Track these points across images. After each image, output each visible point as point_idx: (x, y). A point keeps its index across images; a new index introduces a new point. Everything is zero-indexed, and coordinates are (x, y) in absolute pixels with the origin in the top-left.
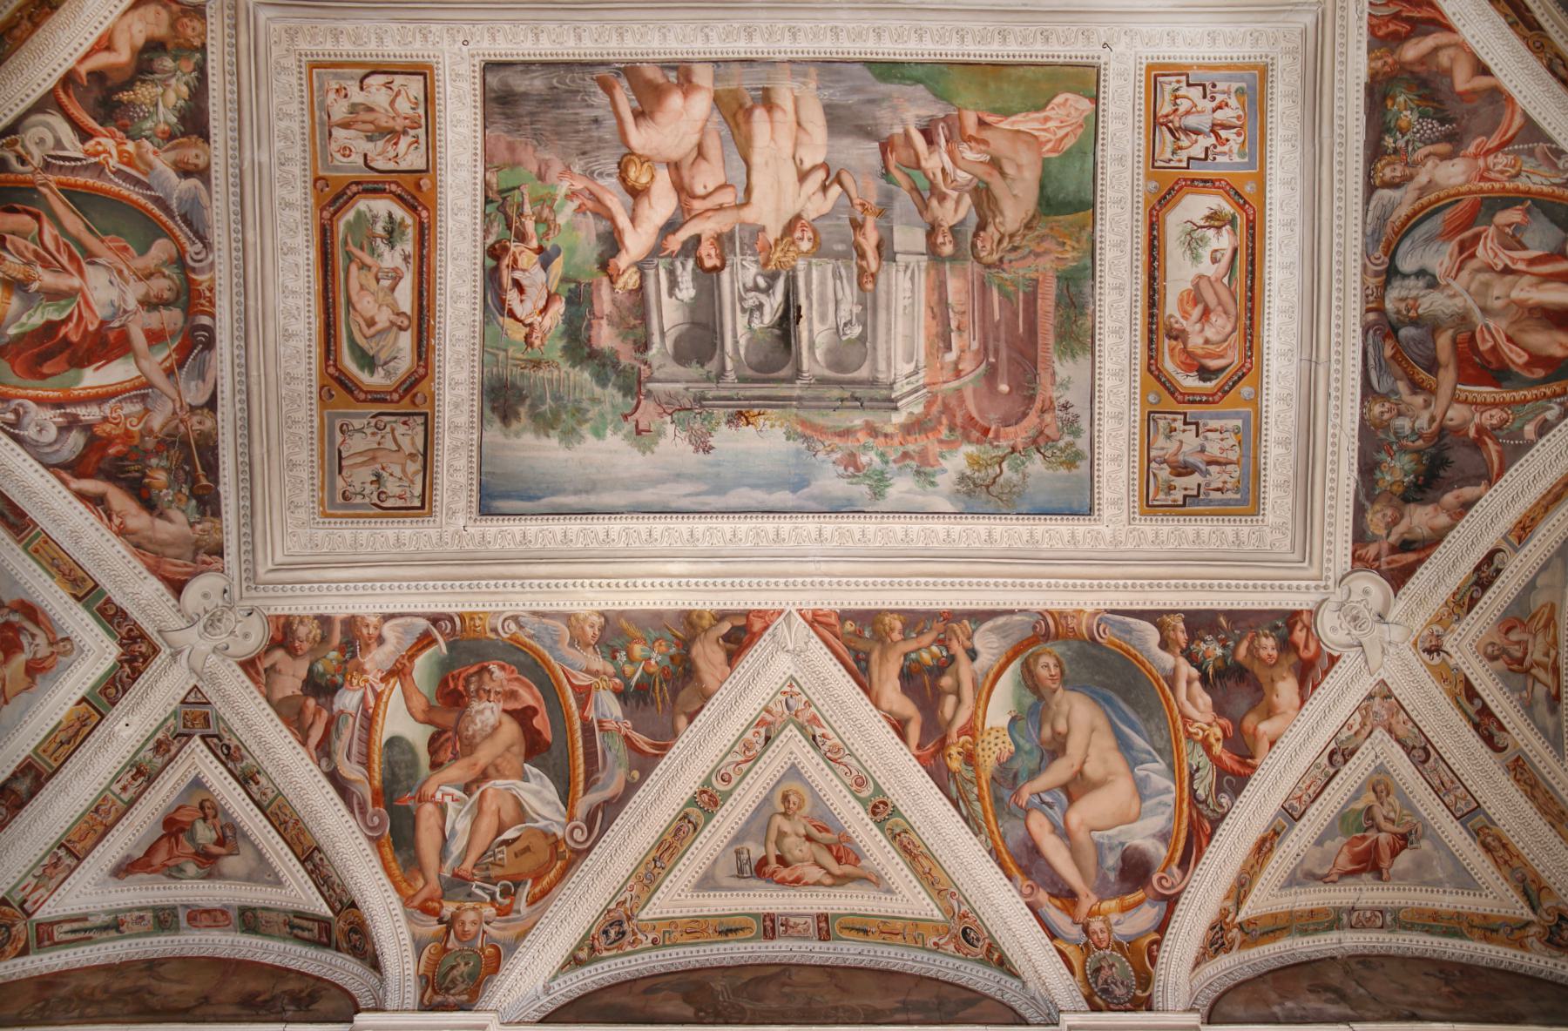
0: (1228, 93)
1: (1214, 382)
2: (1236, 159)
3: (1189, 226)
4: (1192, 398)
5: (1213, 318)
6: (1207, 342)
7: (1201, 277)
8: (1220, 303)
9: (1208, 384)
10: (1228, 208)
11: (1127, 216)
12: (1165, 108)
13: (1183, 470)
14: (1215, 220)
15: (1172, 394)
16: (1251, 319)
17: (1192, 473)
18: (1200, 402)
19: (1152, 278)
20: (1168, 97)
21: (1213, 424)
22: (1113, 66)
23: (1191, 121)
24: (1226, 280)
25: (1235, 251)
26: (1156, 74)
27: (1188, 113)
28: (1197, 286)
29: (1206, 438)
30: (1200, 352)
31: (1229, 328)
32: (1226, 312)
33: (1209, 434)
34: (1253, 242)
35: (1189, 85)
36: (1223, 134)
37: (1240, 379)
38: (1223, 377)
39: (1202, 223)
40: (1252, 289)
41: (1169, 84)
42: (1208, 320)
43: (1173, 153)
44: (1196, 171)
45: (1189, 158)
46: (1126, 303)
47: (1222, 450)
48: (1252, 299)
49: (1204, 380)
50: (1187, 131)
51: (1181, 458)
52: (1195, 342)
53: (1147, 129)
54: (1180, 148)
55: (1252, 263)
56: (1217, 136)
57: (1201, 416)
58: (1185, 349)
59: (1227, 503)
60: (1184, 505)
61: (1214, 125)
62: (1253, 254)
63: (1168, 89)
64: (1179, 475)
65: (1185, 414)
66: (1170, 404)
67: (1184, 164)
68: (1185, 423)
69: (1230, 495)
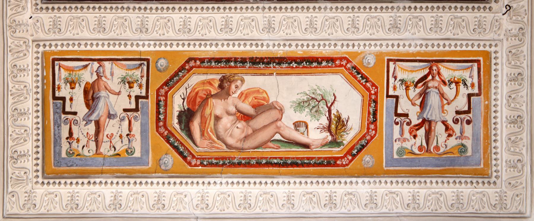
0: (462, 136)
1: (177, 126)
2: (397, 146)
3: (330, 99)
4: (162, 105)
5: (241, 124)
6: (218, 118)
7: (281, 111)
8: (255, 131)
9: (176, 121)
10: (348, 137)
11: (340, 34)
12: (447, 72)
13: (91, 96)
14: (336, 125)
15: (166, 84)
16: (240, 164)
17: (88, 106)
18: (158, 113)
19: (280, 61)
20: (457, 74)
21: (137, 127)
22: (490, 16)
23: (434, 99)
24: (278, 137)
25: (306, 146)
26: (480, 62)
27: (442, 95)
28: (272, 107)
29: (122, 120)
30: (208, 111)
31: (231, 141)
32: (246, 137)
33: (126, 122)
34: (316, 165)
35: (470, 96)
36: (421, 132)
37: (181, 154)
38: (182, 136)
39: (334, 111)
40: (269, 164)
41: (470, 75)
42: (239, 119)
43: (402, 81)
44: (385, 104)
45: (397, 97)
46: (256, 35)
47: (110, 137)
48: (259, 164)
49: (179, 117)
50: (424, 95)
51: (103, 93)
52: (217, 107)
53: (426, 54)
54: (407, 88)
55: (294, 164)
56: (419, 126)
57: (145, 114)
58: (210, 96)
59: (57, 142)
60: (55, 98)
61: (430, 122)
62: (303, 165)
63: (466, 75)
64: (86, 92)
65: (146, 97)
66: (156, 83)
67: (391, 93)
68: (137, 98)
69: (65, 146)
